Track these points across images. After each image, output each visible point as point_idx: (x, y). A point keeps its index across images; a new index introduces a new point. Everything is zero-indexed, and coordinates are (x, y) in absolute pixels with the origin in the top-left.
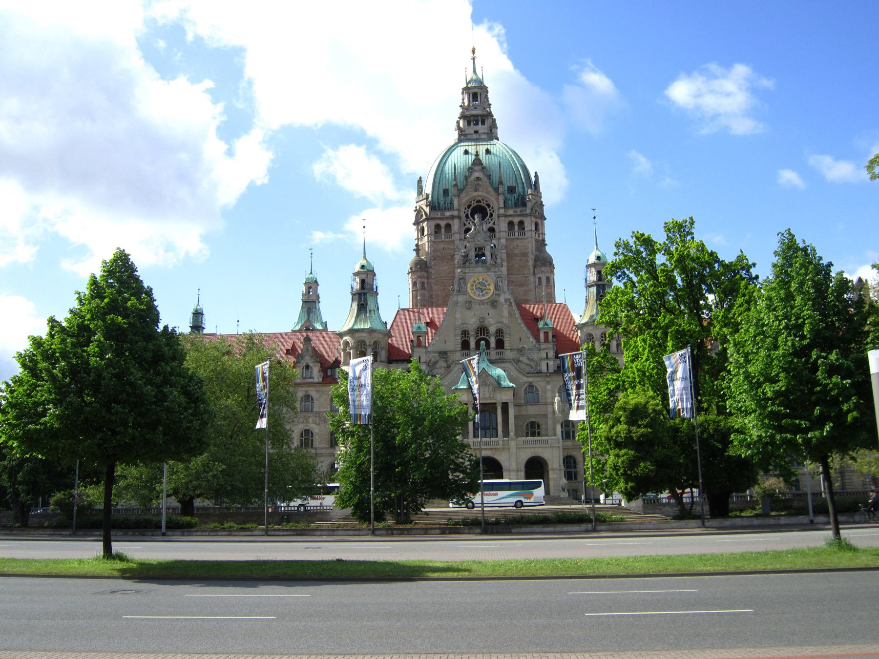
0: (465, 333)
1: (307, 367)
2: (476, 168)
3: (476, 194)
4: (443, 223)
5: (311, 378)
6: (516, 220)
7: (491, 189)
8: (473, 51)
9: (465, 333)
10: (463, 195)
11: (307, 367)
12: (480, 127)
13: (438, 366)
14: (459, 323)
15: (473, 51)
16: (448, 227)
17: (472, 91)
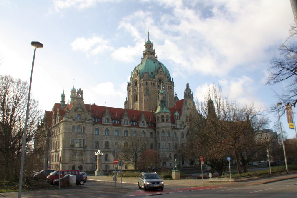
0: (187, 117)
1: (143, 122)
2: (161, 68)
3: (160, 76)
4: (153, 82)
5: (144, 126)
6: (170, 86)
7: (164, 75)
8: (148, 33)
9: (187, 117)
10: (158, 75)
11: (143, 122)
12: (152, 56)
13: (182, 126)
14: (186, 114)
15: (148, 33)
16: (154, 83)
17: (150, 45)
